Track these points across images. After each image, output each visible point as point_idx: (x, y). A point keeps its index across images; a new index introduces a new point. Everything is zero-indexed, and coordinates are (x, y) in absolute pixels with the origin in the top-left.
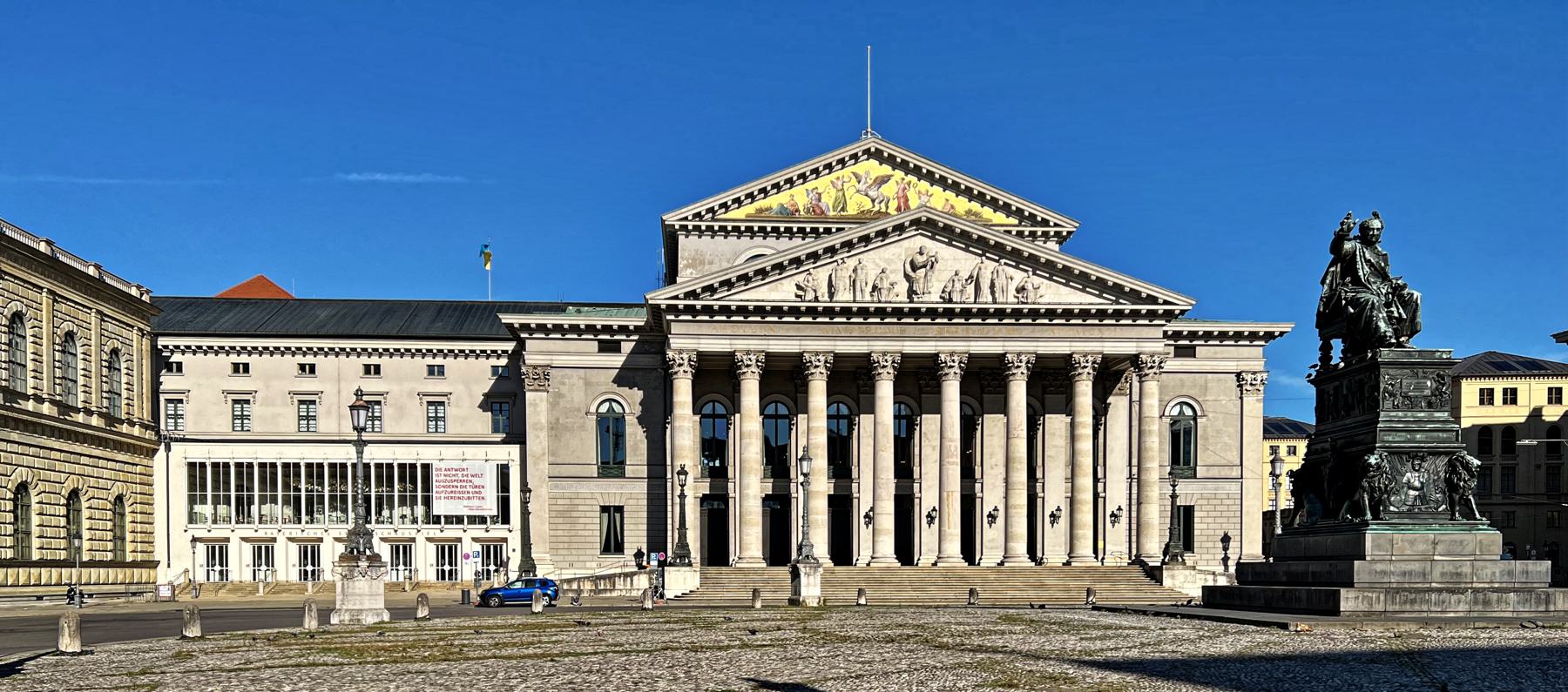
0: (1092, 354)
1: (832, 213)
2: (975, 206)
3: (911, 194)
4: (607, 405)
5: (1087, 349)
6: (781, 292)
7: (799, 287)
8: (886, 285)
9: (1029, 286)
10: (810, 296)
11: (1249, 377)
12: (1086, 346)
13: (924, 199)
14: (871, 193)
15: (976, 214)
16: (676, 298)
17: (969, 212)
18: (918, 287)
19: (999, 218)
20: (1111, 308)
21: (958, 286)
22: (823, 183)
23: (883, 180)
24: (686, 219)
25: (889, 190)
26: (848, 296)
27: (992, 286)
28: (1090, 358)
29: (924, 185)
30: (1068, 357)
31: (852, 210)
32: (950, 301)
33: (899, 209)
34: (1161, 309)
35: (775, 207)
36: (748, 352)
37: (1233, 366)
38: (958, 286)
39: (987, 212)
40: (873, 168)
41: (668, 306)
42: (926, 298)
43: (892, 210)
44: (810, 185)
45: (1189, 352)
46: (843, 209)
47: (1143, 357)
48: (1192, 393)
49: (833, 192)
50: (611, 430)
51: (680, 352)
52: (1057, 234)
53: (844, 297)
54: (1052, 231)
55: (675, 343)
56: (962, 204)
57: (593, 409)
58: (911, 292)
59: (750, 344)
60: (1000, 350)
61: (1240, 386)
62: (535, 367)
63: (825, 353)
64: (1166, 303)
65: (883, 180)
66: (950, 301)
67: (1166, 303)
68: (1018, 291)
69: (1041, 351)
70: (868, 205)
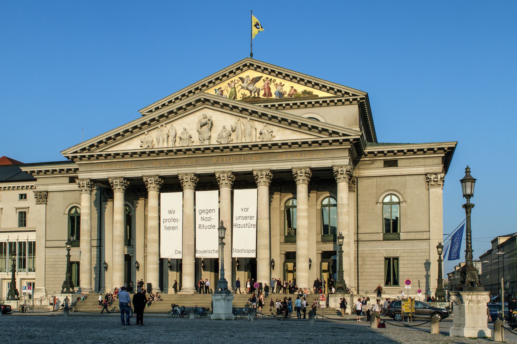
0: (305, 168)
2: (309, 89)
5: (302, 166)
6: (133, 145)
7: (142, 142)
9: (265, 131)
10: (145, 146)
12: (301, 165)
13: (279, 88)
14: (250, 88)
15: (310, 93)
17: (305, 92)
19: (322, 94)
20: (310, 141)
22: (223, 85)
23: (256, 80)
25: (260, 85)
26: (165, 145)
28: (303, 171)
29: (278, 80)
30: (290, 171)
31: (239, 97)
33: (265, 95)
34: (341, 138)
36: (116, 178)
37: (422, 170)
39: (316, 92)
40: (252, 74)
42: (206, 142)
43: (261, 96)
44: (217, 87)
45: (392, 164)
46: (235, 98)
47: (335, 169)
48: (396, 188)
49: (229, 90)
50: (74, 221)
51: (83, 180)
52: (354, 100)
54: (351, 99)
56: (300, 88)
57: (67, 212)
59: (114, 174)
61: (428, 182)
62: (40, 192)
65: (256, 80)
66: (221, 144)
69: (274, 168)
70: (248, 93)
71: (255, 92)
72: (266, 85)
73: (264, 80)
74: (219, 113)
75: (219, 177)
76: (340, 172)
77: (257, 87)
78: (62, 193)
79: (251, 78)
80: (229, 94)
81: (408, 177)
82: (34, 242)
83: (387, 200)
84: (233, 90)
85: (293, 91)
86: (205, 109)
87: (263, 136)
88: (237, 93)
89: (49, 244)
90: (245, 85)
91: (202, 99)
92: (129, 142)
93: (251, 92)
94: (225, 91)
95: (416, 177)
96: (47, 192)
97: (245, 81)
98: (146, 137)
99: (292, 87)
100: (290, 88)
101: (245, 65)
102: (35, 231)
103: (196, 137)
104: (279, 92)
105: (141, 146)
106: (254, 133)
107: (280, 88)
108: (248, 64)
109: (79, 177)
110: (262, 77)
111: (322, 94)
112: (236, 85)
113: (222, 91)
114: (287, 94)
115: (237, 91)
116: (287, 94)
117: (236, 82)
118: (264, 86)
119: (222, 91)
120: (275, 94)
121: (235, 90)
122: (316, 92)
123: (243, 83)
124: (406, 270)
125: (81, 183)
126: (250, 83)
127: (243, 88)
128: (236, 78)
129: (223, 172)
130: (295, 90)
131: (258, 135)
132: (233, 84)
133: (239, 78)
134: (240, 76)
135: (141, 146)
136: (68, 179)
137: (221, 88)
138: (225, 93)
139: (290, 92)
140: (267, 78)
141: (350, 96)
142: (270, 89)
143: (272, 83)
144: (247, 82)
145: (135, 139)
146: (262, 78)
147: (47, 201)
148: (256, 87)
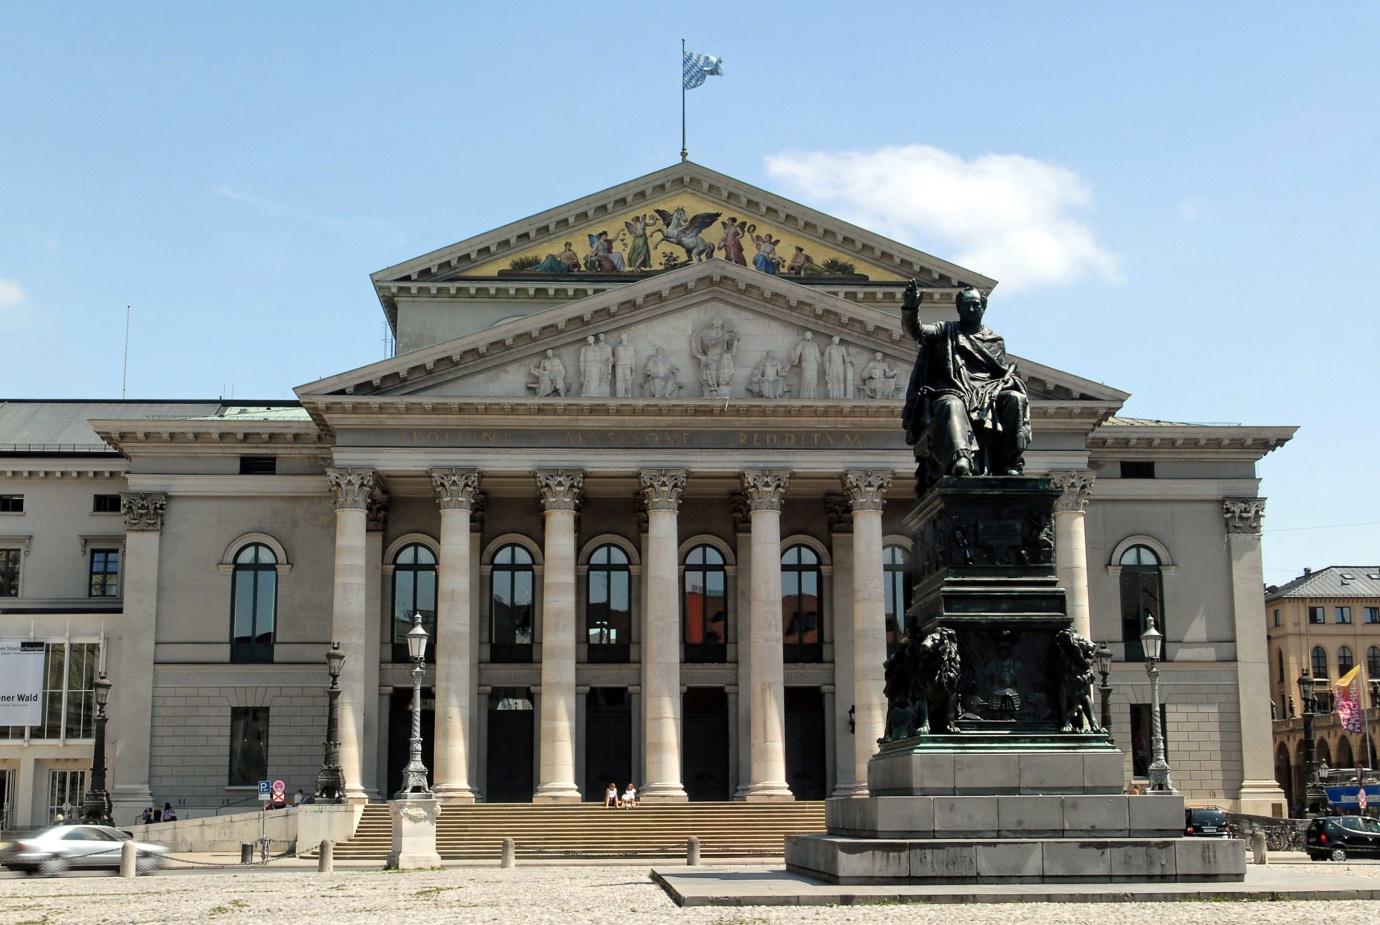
1: (628, 269)
3: (747, 242)
4: (250, 551)
8: (661, 369)
9: (878, 373)
10: (545, 387)
11: (1237, 508)
13: (766, 247)
14: (688, 240)
15: (846, 269)
16: (342, 392)
17: (833, 265)
18: (710, 375)
21: (771, 373)
22: (614, 226)
24: (408, 278)
25: (713, 234)
27: (822, 373)
32: (761, 396)
35: (543, 259)
38: (771, 373)
41: (329, 408)
46: (645, 263)
47: (1056, 479)
49: (629, 240)
53: (596, 390)
55: (341, 457)
57: (230, 559)
58: (702, 385)
60: (839, 468)
62: (145, 496)
63: (570, 473)
64: (1083, 397)
66: (761, 396)
67: (1083, 397)
68: (864, 381)
71: (700, 253)
72: (730, 238)
73: (724, 223)
74: (751, 316)
75: (755, 486)
76: (1066, 489)
77: (707, 240)
78: (214, 504)
79: (690, 215)
80: (628, 250)
81: (1177, 507)
82: (93, 649)
83: (1130, 559)
84: (640, 241)
85: (801, 260)
86: (713, 303)
87: (873, 384)
88: (652, 252)
89: (168, 653)
90: (672, 231)
91: (716, 278)
92: (492, 372)
93: (689, 251)
94: (618, 241)
95: (1197, 506)
96: (168, 498)
97: (674, 222)
98: (547, 364)
99: (801, 250)
100: (794, 251)
101: (681, 180)
102: (119, 611)
103: (687, 375)
104: (765, 259)
105: (529, 388)
106: (850, 376)
107: (768, 249)
108: (687, 179)
109: (337, 463)
110: (718, 215)
111: (875, 274)
112: (649, 231)
113: (610, 242)
114: (787, 264)
115: (651, 247)
116: (787, 264)
117: (648, 221)
118: (725, 240)
119: (610, 242)
120: (755, 263)
121: (646, 243)
122: (861, 268)
123: (668, 225)
124: (1183, 736)
125: (343, 482)
126: (687, 229)
127: (666, 238)
128: (647, 210)
129: (765, 472)
130: (808, 259)
131: (859, 382)
132: (639, 226)
133: (657, 211)
134: (662, 207)
135: (529, 388)
136: (238, 462)
137: (605, 233)
138: (617, 247)
139: (794, 261)
140: (734, 220)
141: (954, 287)
142: (740, 249)
143: (746, 234)
144: (679, 225)
145: (511, 369)
146: (720, 219)
147: (162, 524)
148: (703, 241)
